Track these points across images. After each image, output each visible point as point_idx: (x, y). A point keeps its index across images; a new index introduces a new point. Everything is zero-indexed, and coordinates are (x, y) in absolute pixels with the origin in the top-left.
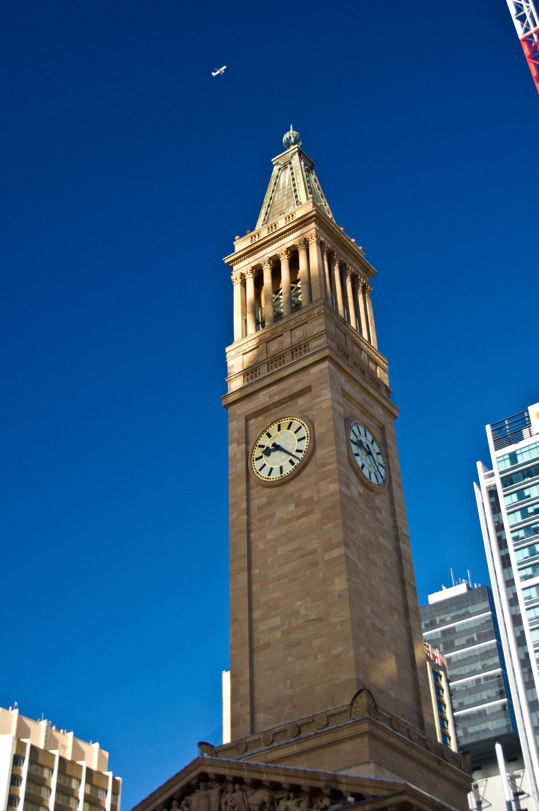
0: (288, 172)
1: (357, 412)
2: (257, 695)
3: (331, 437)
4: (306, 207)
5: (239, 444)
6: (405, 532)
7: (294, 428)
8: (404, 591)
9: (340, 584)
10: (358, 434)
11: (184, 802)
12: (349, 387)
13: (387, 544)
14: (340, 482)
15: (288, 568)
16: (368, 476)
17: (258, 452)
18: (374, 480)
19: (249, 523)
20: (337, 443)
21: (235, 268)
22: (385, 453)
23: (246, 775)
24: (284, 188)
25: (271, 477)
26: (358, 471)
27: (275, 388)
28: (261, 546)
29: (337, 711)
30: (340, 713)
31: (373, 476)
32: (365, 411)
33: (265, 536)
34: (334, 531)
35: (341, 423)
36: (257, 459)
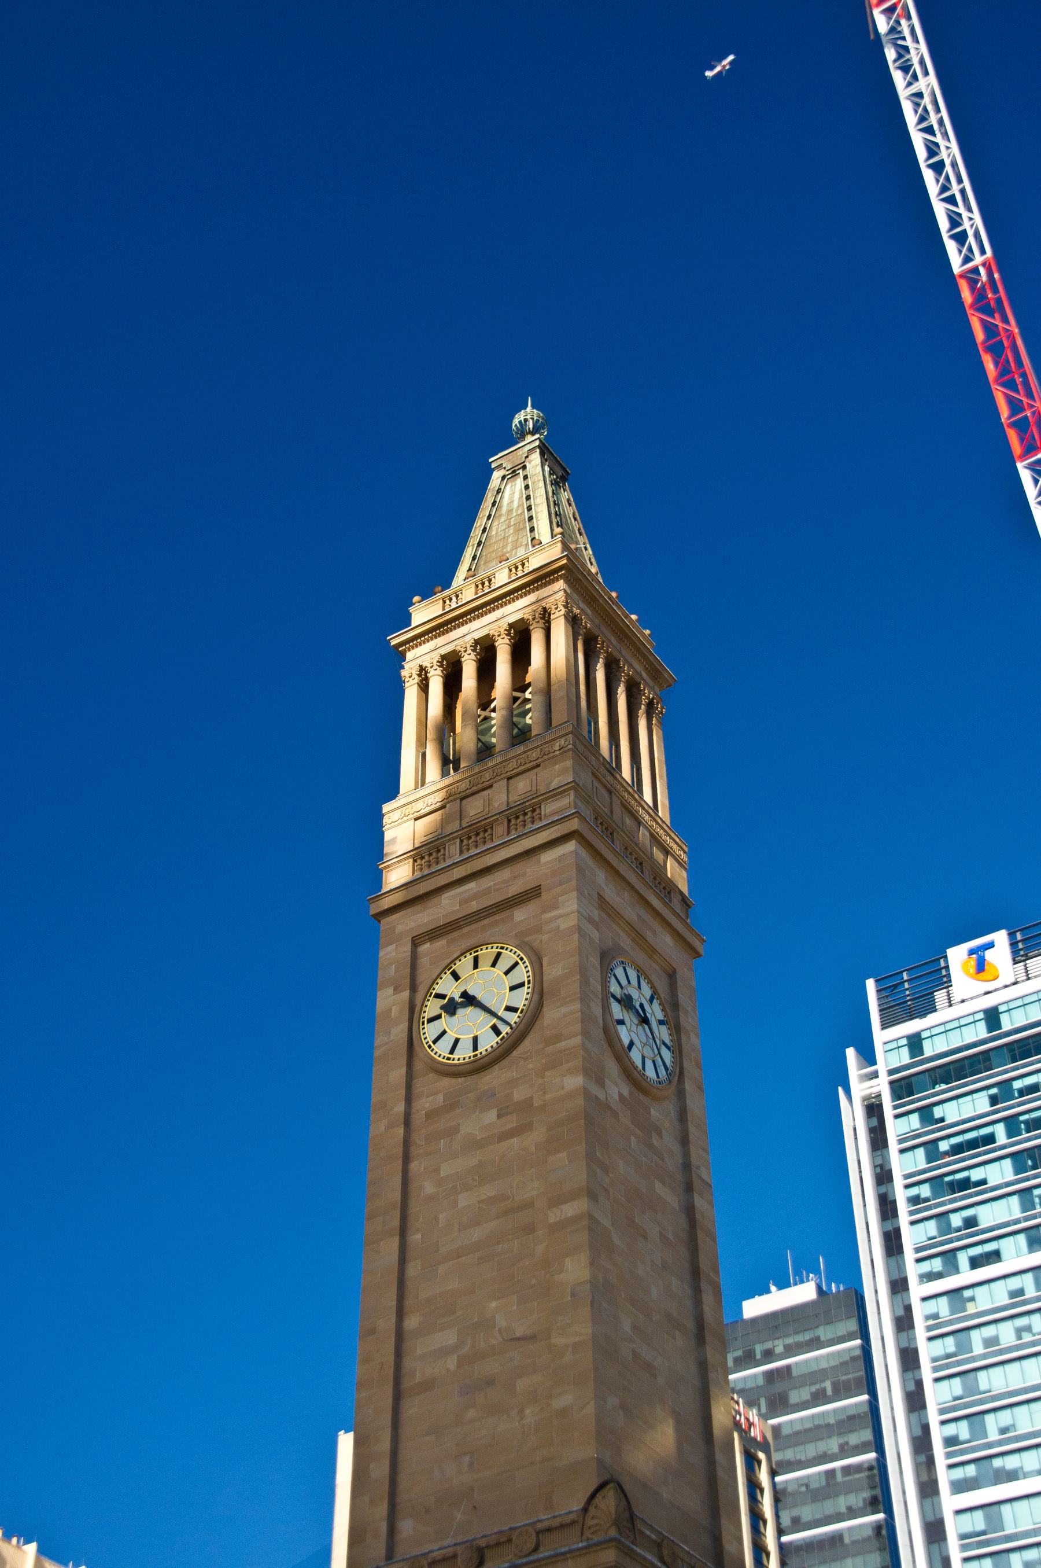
0: (519, 483)
1: (625, 941)
2: (403, 1483)
3: (574, 986)
4: (550, 553)
5: (397, 989)
6: (704, 1174)
7: (504, 964)
8: (697, 1290)
9: (575, 1271)
10: (624, 982)
12: (612, 893)
13: (670, 1197)
14: (586, 1073)
15: (477, 1234)
16: (638, 1063)
17: (433, 1007)
18: (650, 1072)
19: (407, 1144)
20: (584, 999)
21: (409, 655)
22: (673, 1021)
24: (510, 511)
25: (455, 1056)
26: (621, 1054)
27: (471, 886)
28: (429, 1188)
29: (555, 1523)
30: (562, 1526)
31: (649, 1064)
32: (639, 939)
33: (437, 1170)
34: (569, 1167)
35: (594, 960)
36: (430, 1020)
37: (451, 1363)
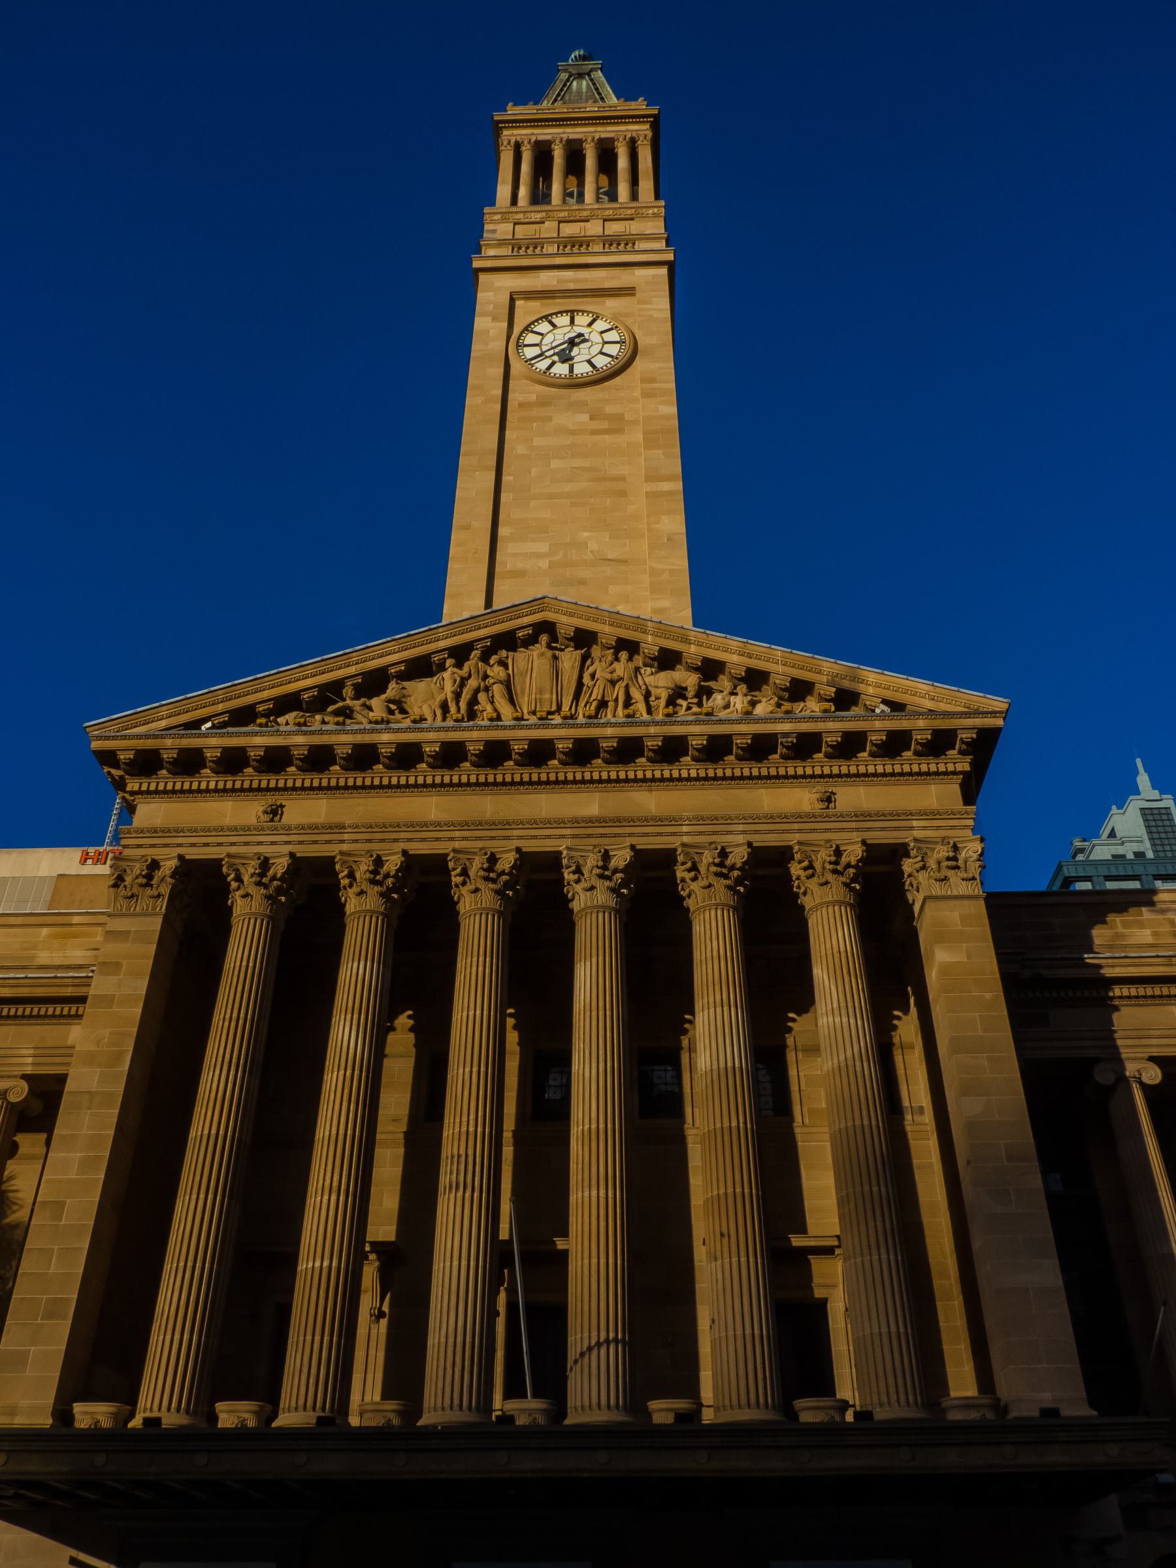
15: (568, 487)
23: (650, 638)
27: (569, 274)
28: (521, 450)
37: (544, 564)
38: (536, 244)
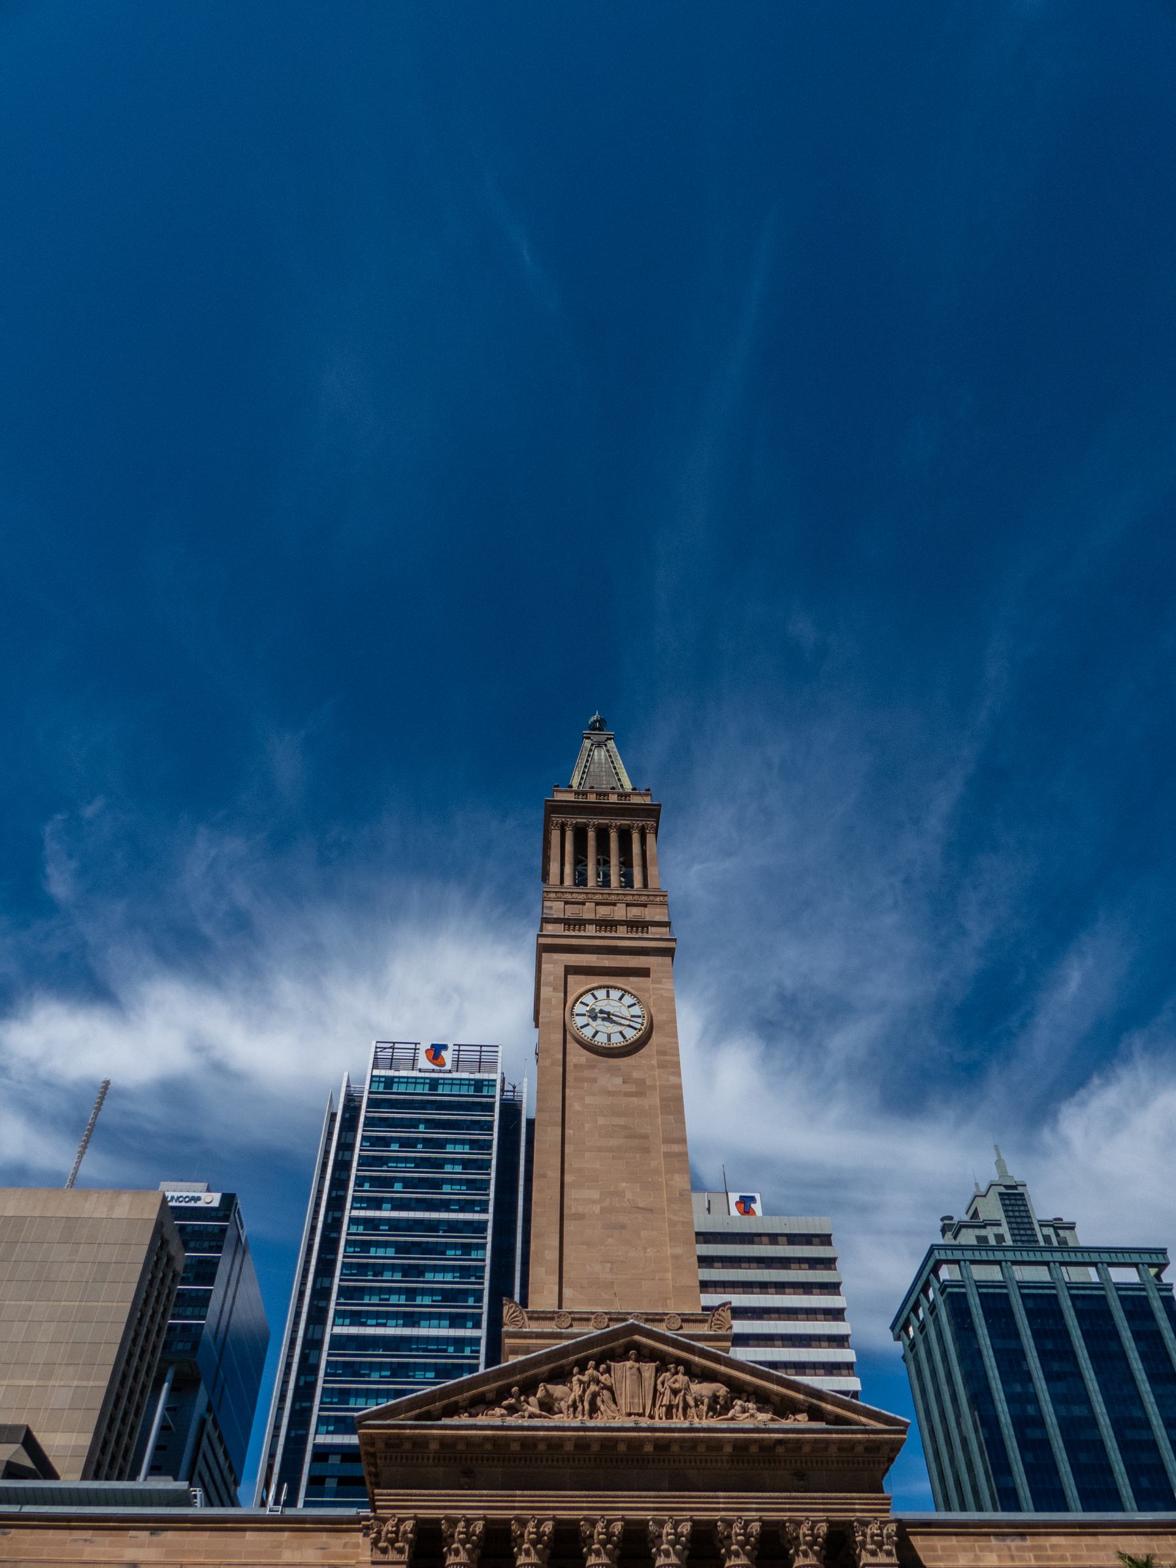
11: (603, 1367)
15: (613, 1142)
37: (596, 1209)
38: (581, 923)
